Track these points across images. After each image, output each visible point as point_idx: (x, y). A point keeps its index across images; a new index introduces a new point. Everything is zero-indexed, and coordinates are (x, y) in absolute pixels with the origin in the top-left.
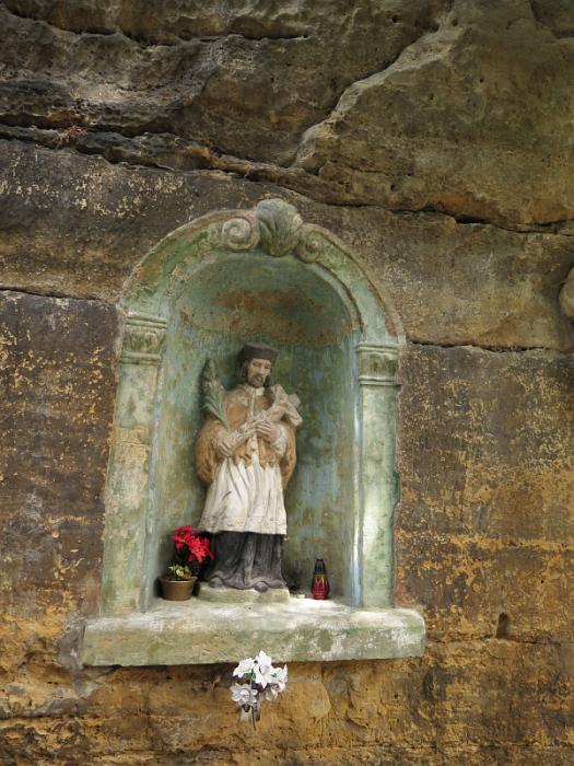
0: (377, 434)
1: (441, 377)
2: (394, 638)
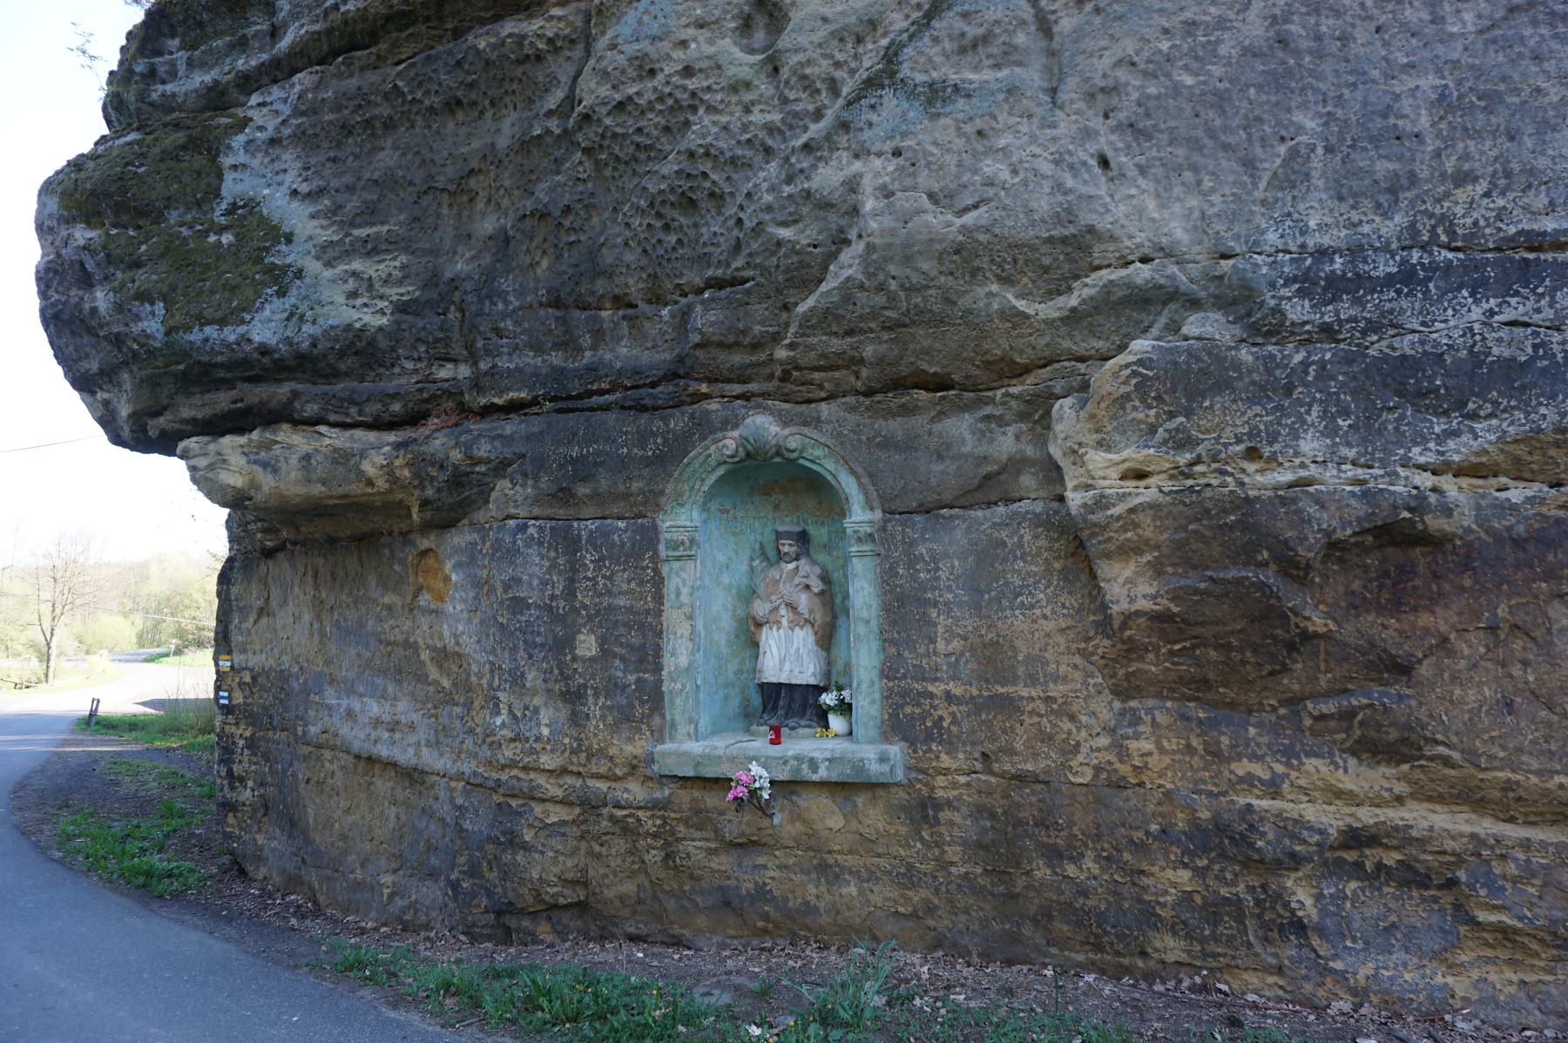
1: (913, 543)
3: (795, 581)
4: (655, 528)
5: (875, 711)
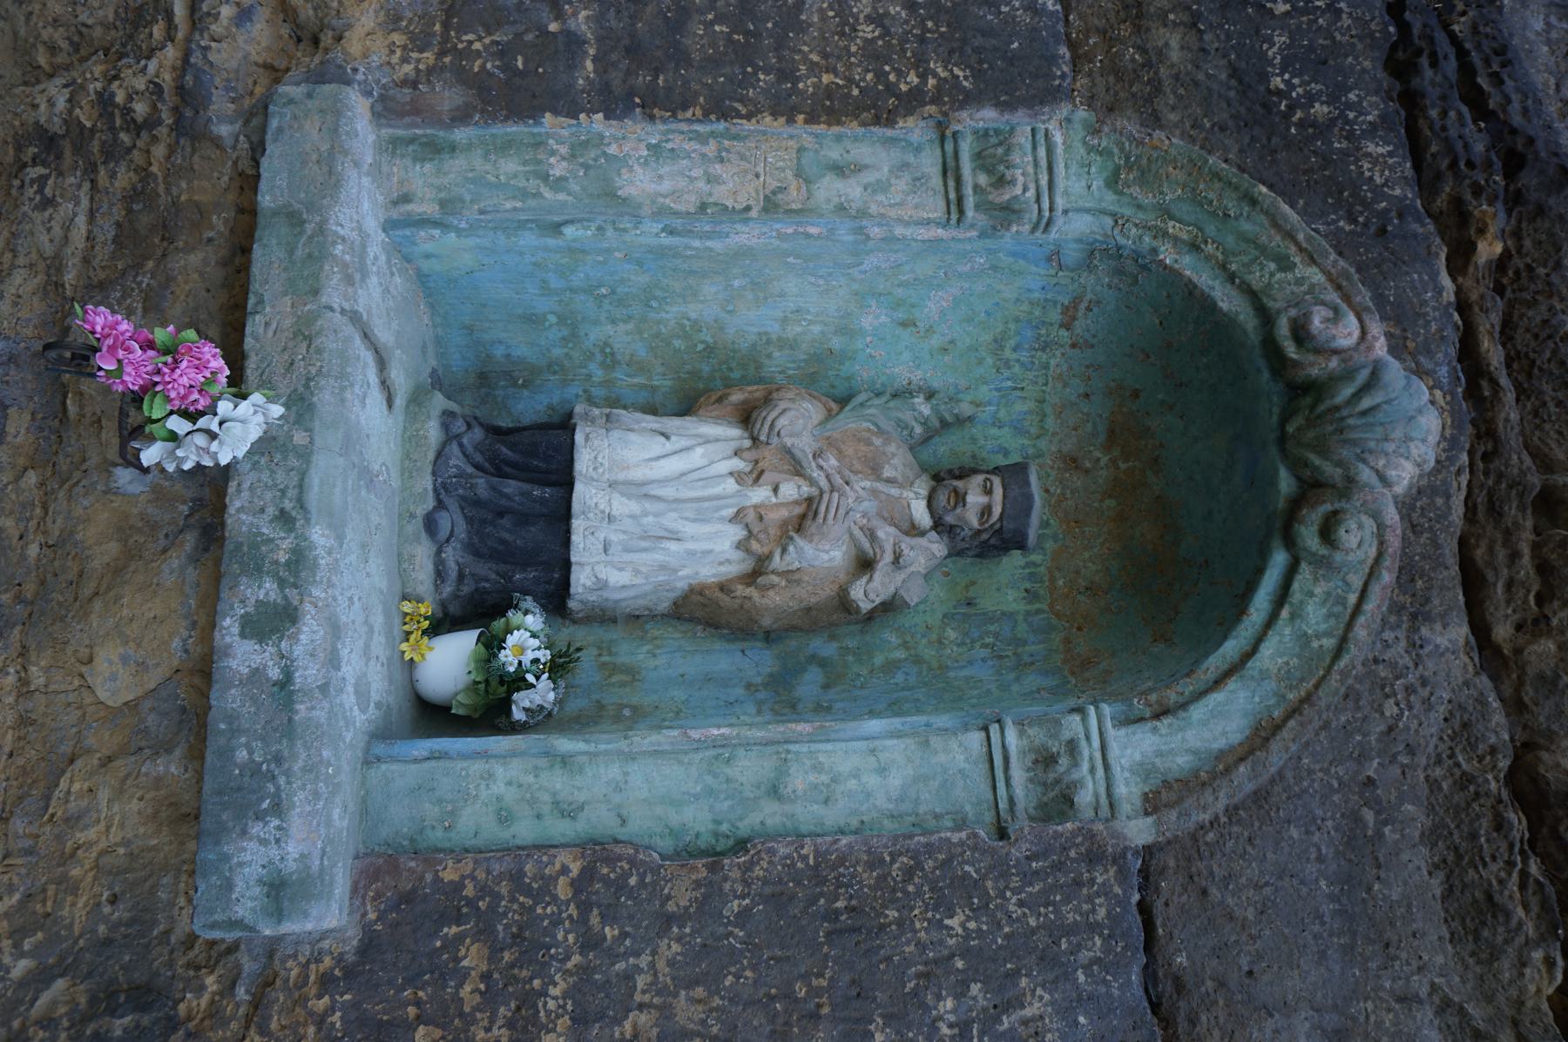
0: (852, 784)
1: (1055, 967)
2: (256, 829)
3: (875, 525)
4: (1046, 96)
5: (475, 822)
